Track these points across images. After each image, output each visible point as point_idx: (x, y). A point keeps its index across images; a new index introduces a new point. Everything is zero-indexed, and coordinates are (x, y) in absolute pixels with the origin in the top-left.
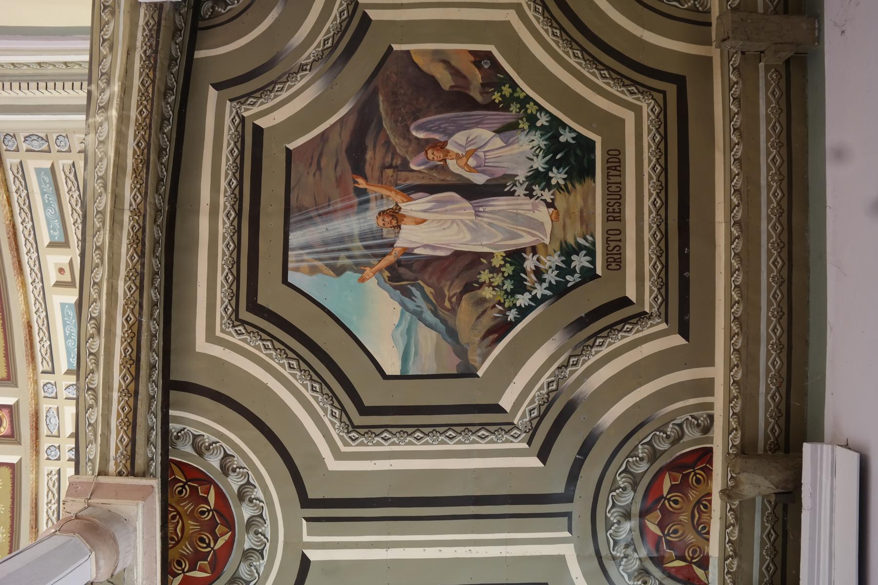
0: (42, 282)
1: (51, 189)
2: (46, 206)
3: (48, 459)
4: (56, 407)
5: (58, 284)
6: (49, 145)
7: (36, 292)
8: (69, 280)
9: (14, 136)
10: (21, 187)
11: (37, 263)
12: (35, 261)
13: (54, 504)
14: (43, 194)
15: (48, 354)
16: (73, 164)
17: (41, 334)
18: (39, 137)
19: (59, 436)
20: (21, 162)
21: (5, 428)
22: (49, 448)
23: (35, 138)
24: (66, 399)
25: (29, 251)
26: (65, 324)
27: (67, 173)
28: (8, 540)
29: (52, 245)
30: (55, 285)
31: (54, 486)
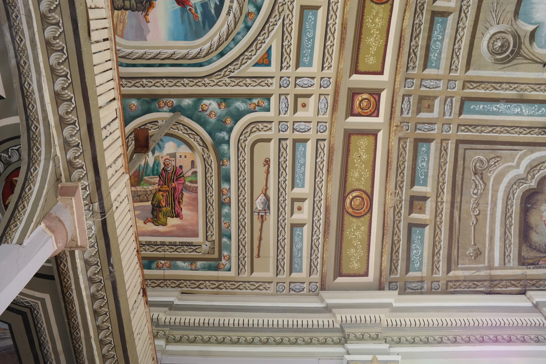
0: (314, 201)
1: (296, 260)
2: (301, 250)
3: (329, 78)
4: (319, 116)
5: (303, 200)
7: (320, 194)
8: (295, 203)
9: (309, 291)
12: (316, 214)
13: (328, 45)
14: (301, 257)
15: (319, 152)
16: (277, 275)
18: (295, 291)
19: (320, 95)
20: (310, 276)
21: (358, 99)
22: (328, 86)
23: (297, 290)
24: (311, 122)
26: (304, 174)
27: (282, 270)
28: (365, 17)
30: (306, 199)
31: (328, 58)
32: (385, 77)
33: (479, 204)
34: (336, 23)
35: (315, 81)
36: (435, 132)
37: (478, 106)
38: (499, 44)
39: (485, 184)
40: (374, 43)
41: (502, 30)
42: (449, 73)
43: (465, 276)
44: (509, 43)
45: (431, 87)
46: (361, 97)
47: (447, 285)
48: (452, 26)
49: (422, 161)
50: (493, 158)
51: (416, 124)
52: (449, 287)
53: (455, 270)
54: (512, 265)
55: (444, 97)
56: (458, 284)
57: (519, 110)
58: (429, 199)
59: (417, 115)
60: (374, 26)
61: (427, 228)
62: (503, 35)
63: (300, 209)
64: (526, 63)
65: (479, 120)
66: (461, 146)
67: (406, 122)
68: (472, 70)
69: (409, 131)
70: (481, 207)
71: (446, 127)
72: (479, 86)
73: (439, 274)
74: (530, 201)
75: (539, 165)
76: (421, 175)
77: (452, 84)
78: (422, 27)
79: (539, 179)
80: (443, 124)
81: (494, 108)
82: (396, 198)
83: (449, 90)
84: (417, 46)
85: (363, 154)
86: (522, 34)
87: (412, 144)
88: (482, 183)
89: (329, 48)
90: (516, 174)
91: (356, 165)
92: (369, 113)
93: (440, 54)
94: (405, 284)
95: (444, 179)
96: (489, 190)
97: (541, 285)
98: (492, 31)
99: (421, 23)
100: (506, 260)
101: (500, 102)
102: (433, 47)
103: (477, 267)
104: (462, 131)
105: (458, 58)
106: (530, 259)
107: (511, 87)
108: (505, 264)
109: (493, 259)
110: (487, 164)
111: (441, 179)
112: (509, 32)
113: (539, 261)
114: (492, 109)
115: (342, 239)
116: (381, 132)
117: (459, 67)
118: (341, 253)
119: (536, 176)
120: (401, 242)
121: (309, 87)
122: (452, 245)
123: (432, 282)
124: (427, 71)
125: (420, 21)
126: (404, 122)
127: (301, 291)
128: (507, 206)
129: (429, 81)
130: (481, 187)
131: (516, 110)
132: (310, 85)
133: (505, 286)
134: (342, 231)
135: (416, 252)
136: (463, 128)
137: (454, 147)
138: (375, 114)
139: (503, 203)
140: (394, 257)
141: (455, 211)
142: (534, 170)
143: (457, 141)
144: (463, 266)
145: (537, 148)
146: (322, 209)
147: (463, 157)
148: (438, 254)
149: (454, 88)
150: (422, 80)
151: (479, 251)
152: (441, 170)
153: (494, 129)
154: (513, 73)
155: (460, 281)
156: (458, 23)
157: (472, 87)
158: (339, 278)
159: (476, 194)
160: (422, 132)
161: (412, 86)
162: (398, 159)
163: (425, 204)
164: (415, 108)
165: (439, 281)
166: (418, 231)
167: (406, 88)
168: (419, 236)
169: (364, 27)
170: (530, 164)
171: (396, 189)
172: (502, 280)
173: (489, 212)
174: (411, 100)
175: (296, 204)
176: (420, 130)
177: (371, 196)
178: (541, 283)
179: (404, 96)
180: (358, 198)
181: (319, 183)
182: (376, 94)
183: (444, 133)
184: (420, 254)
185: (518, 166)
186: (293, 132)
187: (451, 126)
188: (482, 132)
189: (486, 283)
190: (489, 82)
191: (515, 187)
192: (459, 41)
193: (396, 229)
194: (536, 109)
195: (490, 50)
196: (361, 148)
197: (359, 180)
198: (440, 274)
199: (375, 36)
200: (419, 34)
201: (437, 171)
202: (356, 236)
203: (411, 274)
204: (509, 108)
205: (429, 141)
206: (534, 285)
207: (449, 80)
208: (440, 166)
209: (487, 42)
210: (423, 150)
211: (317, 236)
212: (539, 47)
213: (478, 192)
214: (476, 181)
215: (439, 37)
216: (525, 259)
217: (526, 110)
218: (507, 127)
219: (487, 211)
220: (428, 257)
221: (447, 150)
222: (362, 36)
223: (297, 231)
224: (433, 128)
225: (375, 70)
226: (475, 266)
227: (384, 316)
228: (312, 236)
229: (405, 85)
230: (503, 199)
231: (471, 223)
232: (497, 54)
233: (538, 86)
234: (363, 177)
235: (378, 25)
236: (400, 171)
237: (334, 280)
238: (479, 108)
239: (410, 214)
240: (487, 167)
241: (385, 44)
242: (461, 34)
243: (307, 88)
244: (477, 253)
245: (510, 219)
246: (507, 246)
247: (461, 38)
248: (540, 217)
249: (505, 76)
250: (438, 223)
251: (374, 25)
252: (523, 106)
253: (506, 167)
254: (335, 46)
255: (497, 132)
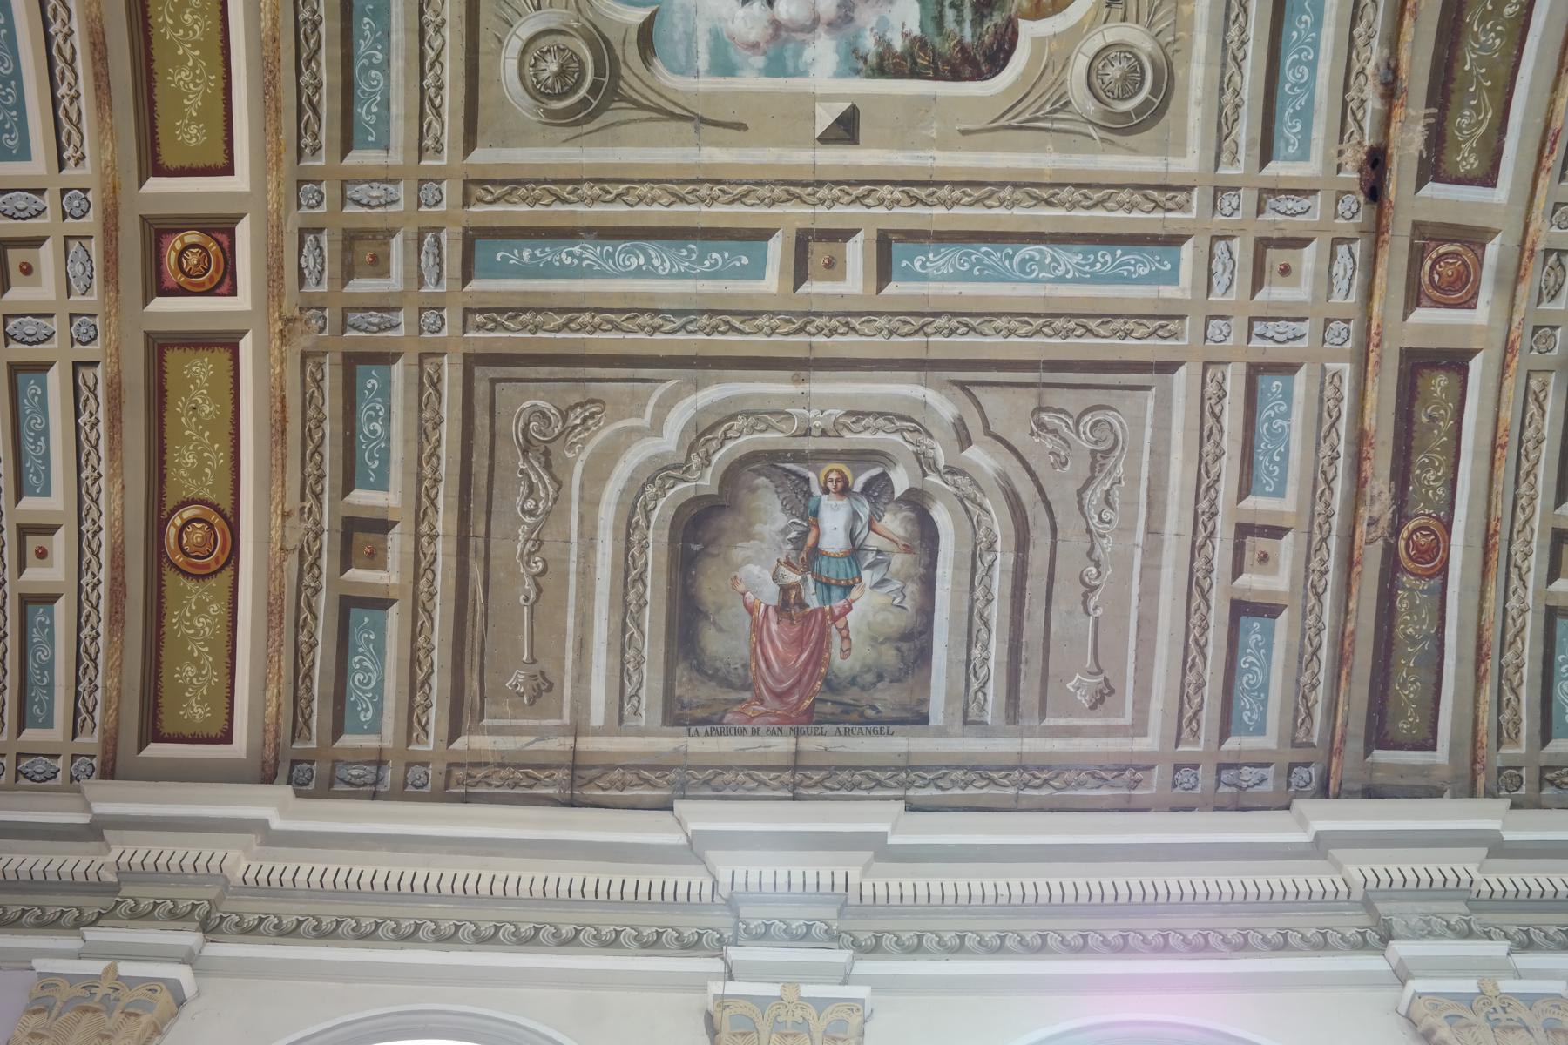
0: (80, 533)
1: (36, 694)
2: (49, 666)
3: (85, 191)
4: (72, 298)
5: (50, 530)
6: (17, 765)
7: (94, 513)
8: (29, 539)
10: (86, 696)
11: (84, 567)
13: (63, 97)
14: (50, 687)
15: (82, 399)
17: (93, 436)
18: (31, 779)
19: (67, 238)
20: (74, 736)
21: (173, 248)
22: (85, 213)
23: (38, 777)
24: (52, 315)
25: (95, 587)
26: (46, 458)
28: (151, 11)
29: (50, 599)
30: (57, 528)
31: (69, 134)
32: (240, 181)
33: (542, 543)
34: (72, 32)
35: (46, 201)
36: (401, 332)
37: (516, 252)
38: (553, 66)
39: (559, 484)
40: (191, 86)
41: (553, 25)
42: (420, 160)
43: (502, 753)
44: (581, 64)
45: (374, 203)
46: (181, 239)
47: (449, 774)
48: (406, 21)
49: (370, 419)
50: (577, 405)
51: (346, 311)
52: (453, 782)
53: (471, 732)
54: (642, 723)
55: (412, 230)
56: (481, 773)
57: (642, 261)
58: (397, 528)
59: (344, 285)
60: (184, 36)
61: (393, 611)
62: (560, 39)
63: (42, 554)
64: (641, 120)
65: (525, 293)
66: (478, 372)
67: (317, 308)
68: (483, 147)
69: (326, 333)
70: (549, 550)
71: (430, 318)
72: (510, 194)
73: (427, 744)
74: (700, 533)
75: (719, 423)
76: (372, 458)
77: (429, 191)
78: (323, 29)
79: (724, 467)
80: (421, 310)
81: (564, 256)
82: (303, 525)
83: (424, 209)
84: (318, 87)
85: (204, 402)
86: (614, 36)
87: (340, 371)
88: (547, 481)
89: (67, 104)
90: (652, 451)
91: (187, 433)
92: (208, 286)
93: (386, 104)
94: (333, 769)
95: (436, 470)
96: (570, 500)
97: (727, 784)
98: (525, 30)
99: (316, 17)
100: (628, 708)
101: (581, 238)
102: (364, 86)
103: (536, 728)
104: (480, 327)
105: (439, 114)
106: (698, 707)
107: (608, 192)
108: (621, 720)
109: (588, 704)
110: (560, 424)
111: (427, 470)
112: (576, 30)
113: (725, 711)
114: (560, 260)
115: (159, 638)
116: (248, 337)
117: (445, 140)
118: (158, 677)
119: (715, 459)
120: (319, 649)
121: (32, 217)
122: (463, 660)
123: (409, 765)
124: (355, 158)
125: (314, 12)
126: (309, 309)
127: (47, 779)
128: (628, 549)
129: (365, 186)
130: (546, 490)
131: (633, 262)
132: (34, 213)
133: (618, 784)
134: (160, 615)
135: (362, 678)
136: (480, 319)
137: (460, 374)
138: (224, 288)
139: (615, 539)
140: (302, 692)
141: (471, 561)
142: (707, 440)
143: (466, 356)
144: (496, 722)
145: (713, 373)
146: (102, 555)
147: (487, 402)
148: (426, 687)
149: (437, 203)
150: (344, 183)
151: (545, 679)
152: (425, 443)
153: (571, 320)
154: (608, 150)
155: (487, 764)
156: (422, 13)
157: (489, 198)
158: (152, 746)
159: (531, 513)
160: (364, 334)
161: (319, 203)
162: (304, 413)
163: (385, 540)
164: (338, 268)
165: (426, 764)
166: (366, 620)
167: (304, 210)
168: (369, 634)
169: (155, 40)
170: (693, 424)
171: (303, 498)
172: (613, 767)
173: (573, 567)
174: (325, 244)
175: (33, 542)
176: (357, 329)
177: (232, 519)
178: (728, 776)
179: (302, 233)
180: (199, 526)
181: (89, 482)
182: (222, 231)
183: (427, 335)
184: (373, 683)
185: (657, 428)
186: (7, 345)
187: (445, 313)
188: (537, 328)
189: (560, 775)
190: (537, 182)
191: (651, 491)
192: (432, 65)
193: (305, 613)
194: (694, 257)
195: (530, 86)
196: (195, 384)
197: (197, 473)
198: (429, 745)
199: (190, 64)
200: (316, 52)
201: (414, 446)
202: (198, 631)
203: (348, 740)
204: (610, 255)
205: (385, 359)
206: (706, 783)
207: (422, 181)
208: (423, 432)
209: (515, 62)
210: (370, 386)
211: (93, 628)
212: (674, 72)
213: (537, 506)
214: (531, 474)
215: (374, 55)
216: (683, 707)
217: (663, 261)
218: (611, 311)
219: (567, 561)
220: (398, 693)
221: (439, 386)
222: (156, 66)
223: (38, 615)
224: (394, 323)
225: (210, 162)
226: (532, 722)
227: (238, 859)
228: (79, 629)
229: (299, 200)
230: (616, 529)
231: (523, 597)
232: (550, 97)
233: (690, 188)
234: (209, 467)
235: (195, 32)
236: (311, 447)
237: (140, 749)
238: (521, 257)
239: (344, 570)
240: (561, 434)
241: (222, 85)
242: (437, 44)
243: (28, 221)
244: (538, 685)
245: (640, 585)
246: (630, 667)
247: (438, 55)
248: (729, 582)
249: (584, 160)
250: (424, 597)
251: (181, 31)
252: (652, 248)
253: (618, 433)
254: (82, 98)
255: (582, 328)
